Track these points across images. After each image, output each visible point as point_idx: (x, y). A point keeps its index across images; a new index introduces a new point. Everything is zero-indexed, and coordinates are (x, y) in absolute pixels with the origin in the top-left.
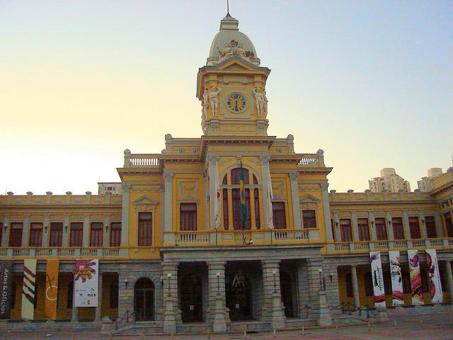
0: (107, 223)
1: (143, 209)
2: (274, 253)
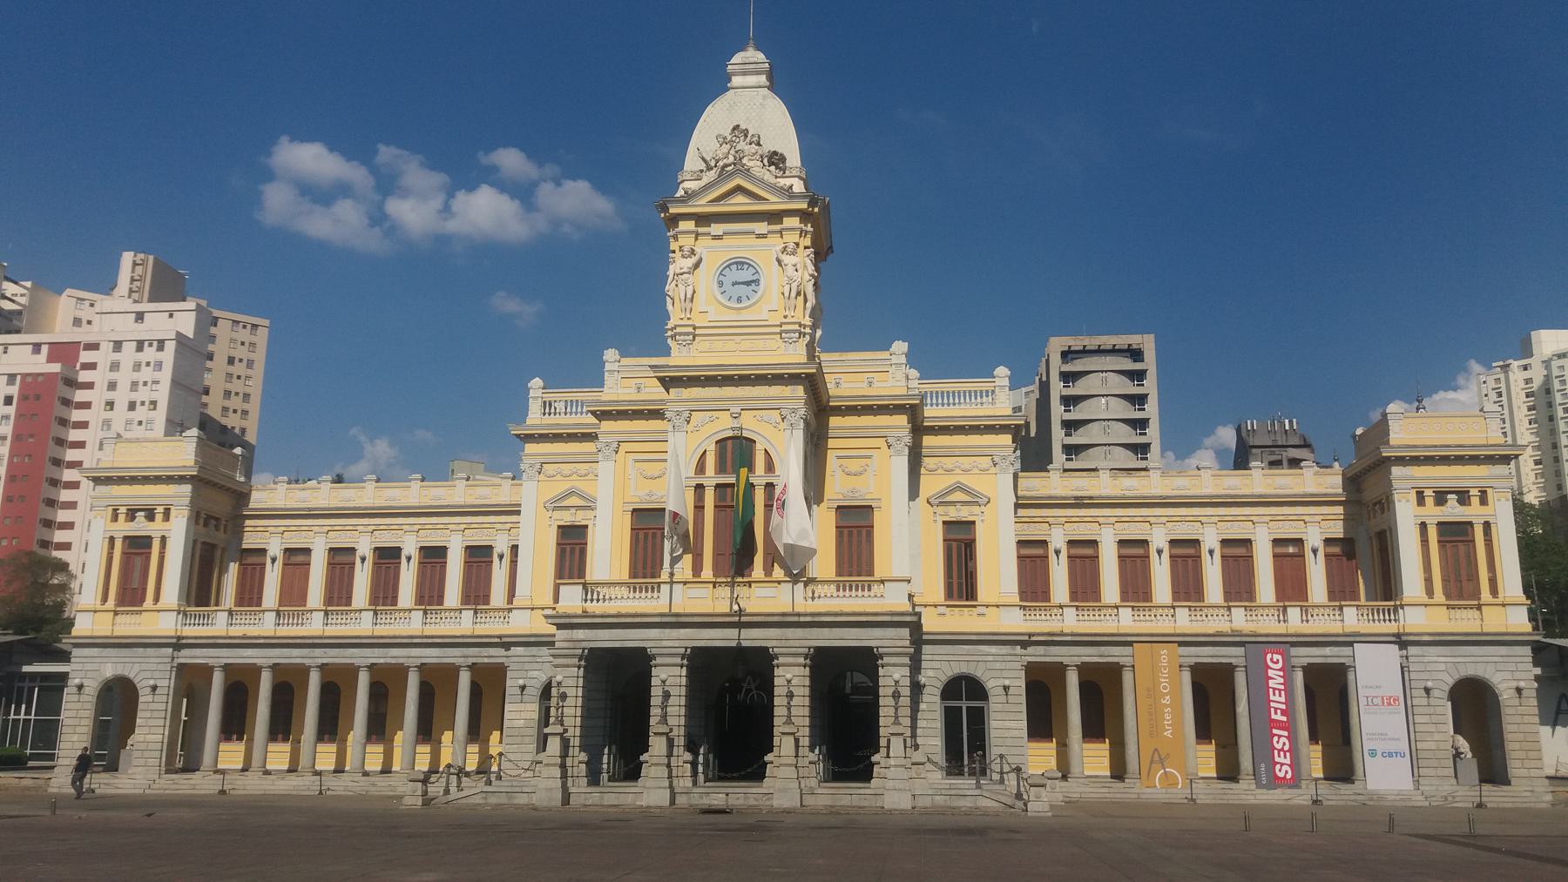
1: (567, 518)
2: (799, 632)
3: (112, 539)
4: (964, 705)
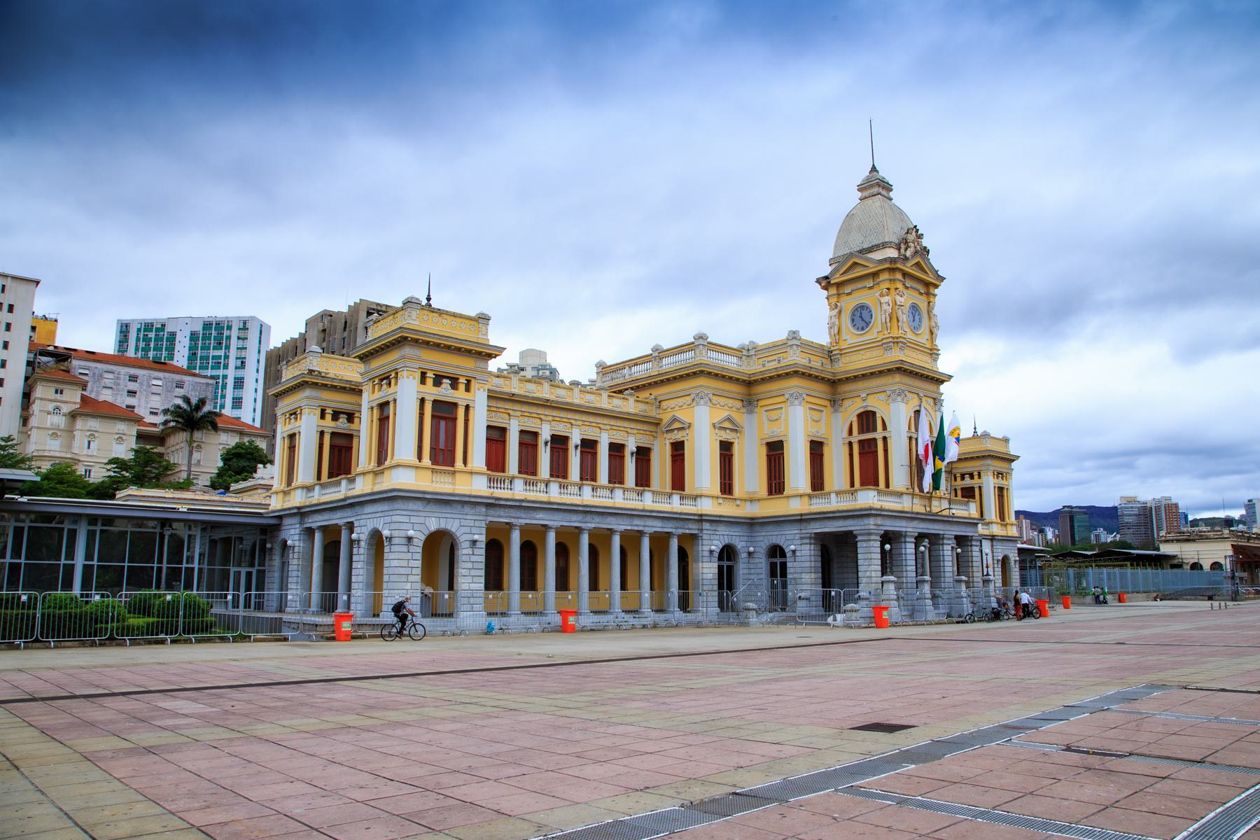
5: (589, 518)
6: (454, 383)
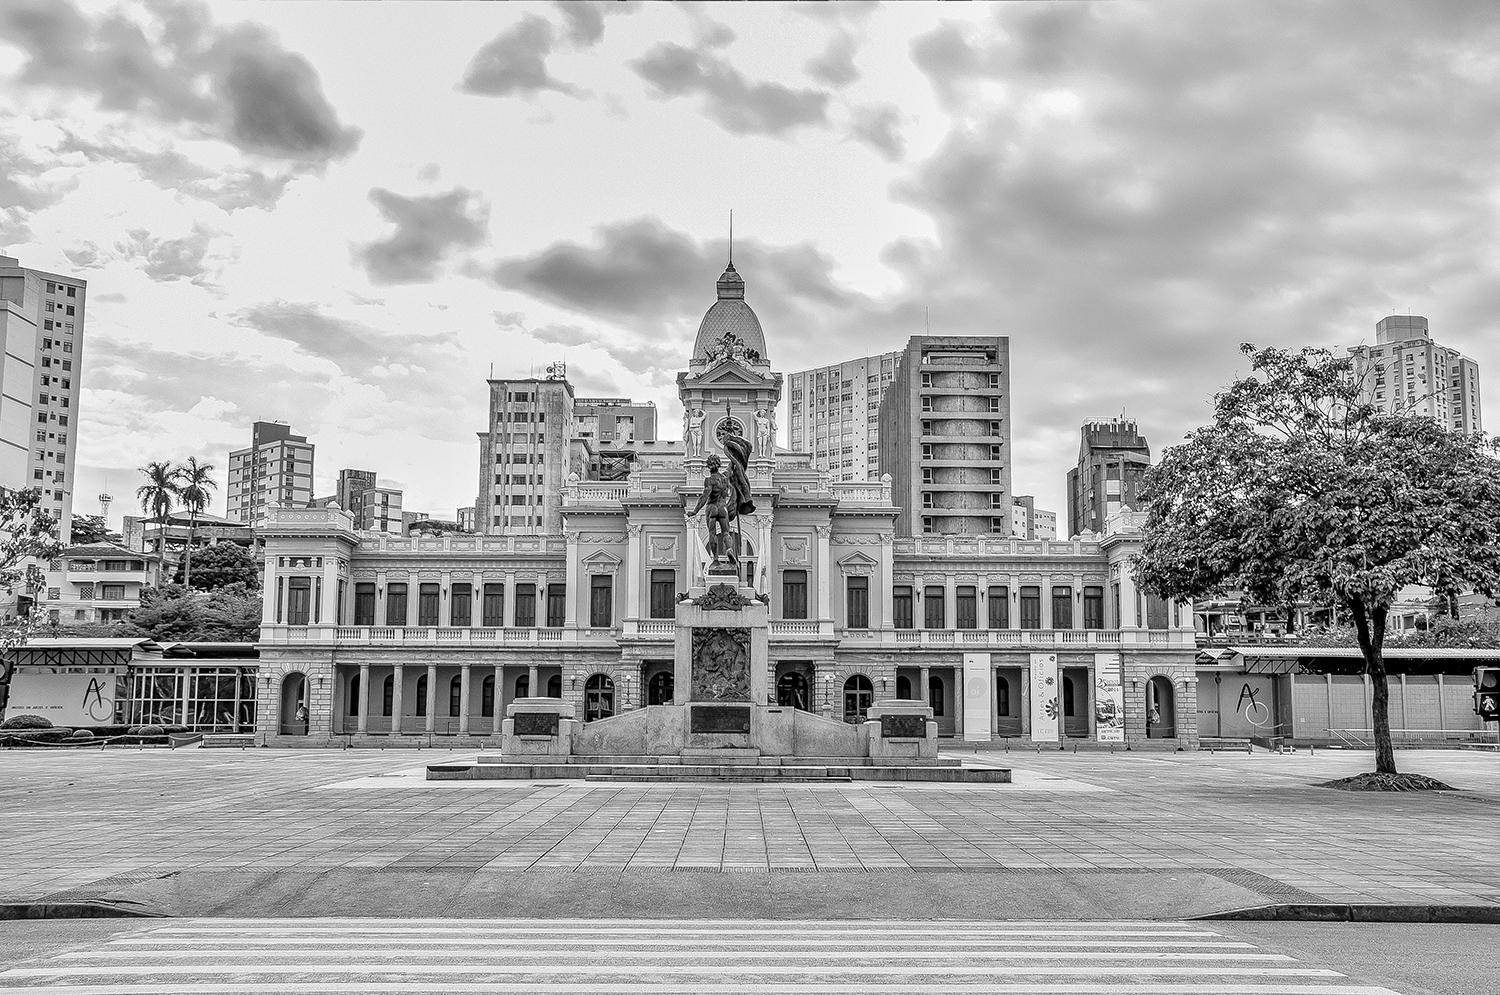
0: (542, 584)
1: (599, 570)
3: (281, 578)
4: (858, 692)
5: (433, 656)
6: (307, 561)
